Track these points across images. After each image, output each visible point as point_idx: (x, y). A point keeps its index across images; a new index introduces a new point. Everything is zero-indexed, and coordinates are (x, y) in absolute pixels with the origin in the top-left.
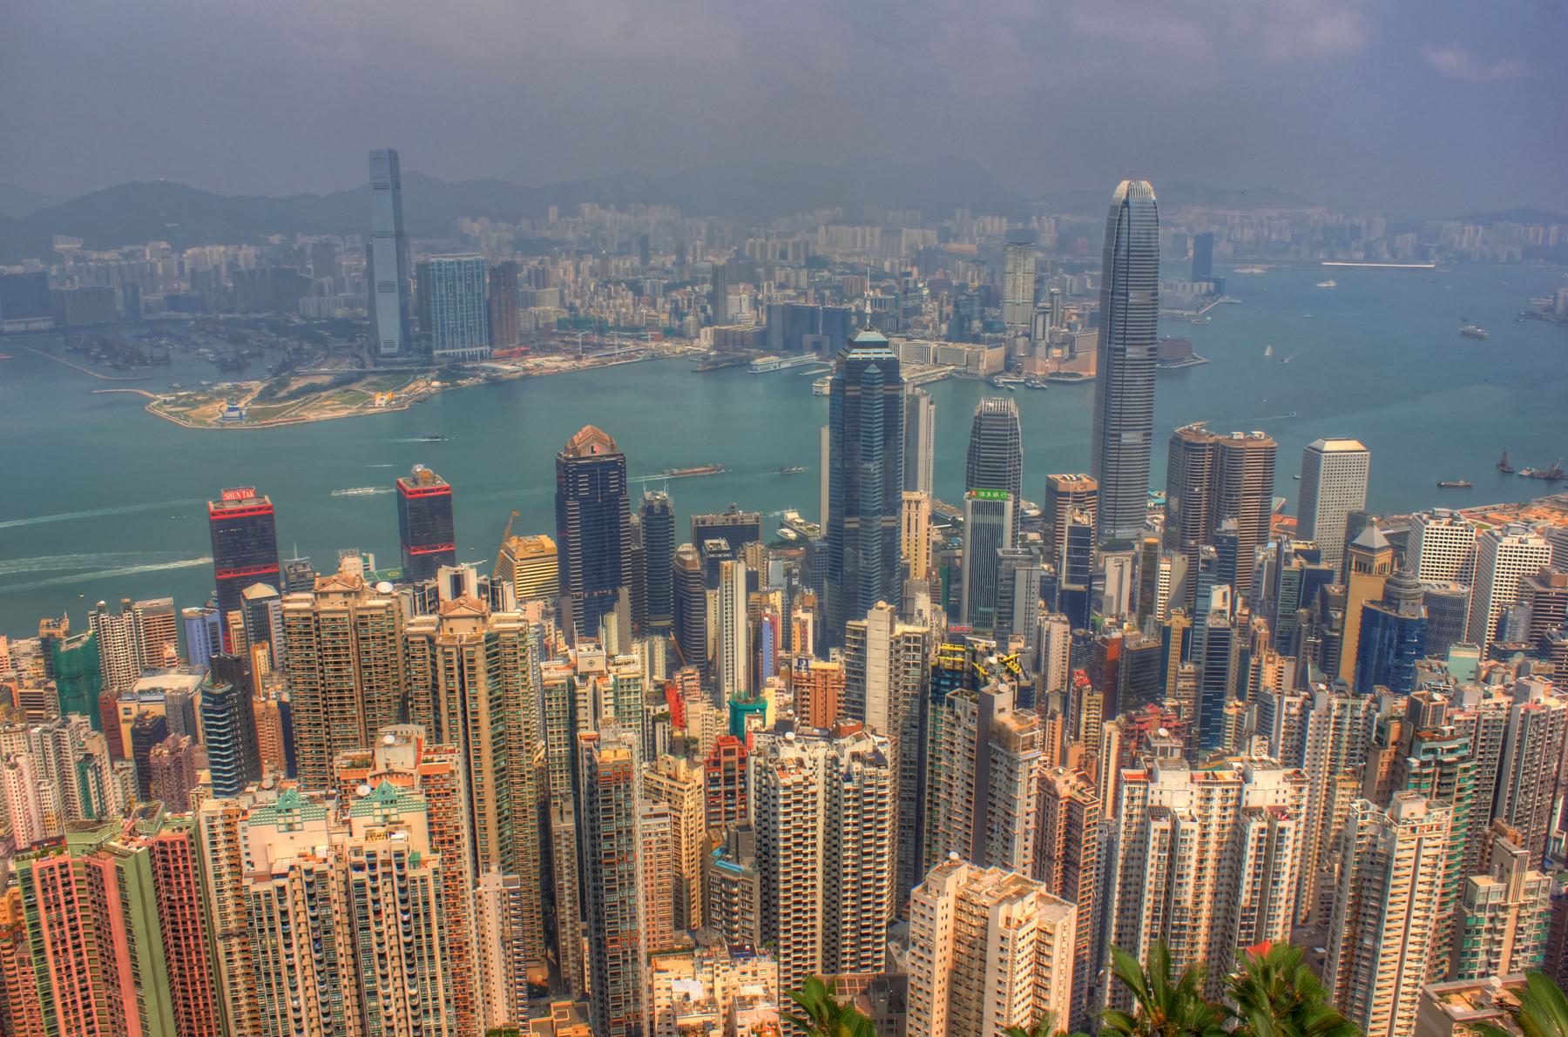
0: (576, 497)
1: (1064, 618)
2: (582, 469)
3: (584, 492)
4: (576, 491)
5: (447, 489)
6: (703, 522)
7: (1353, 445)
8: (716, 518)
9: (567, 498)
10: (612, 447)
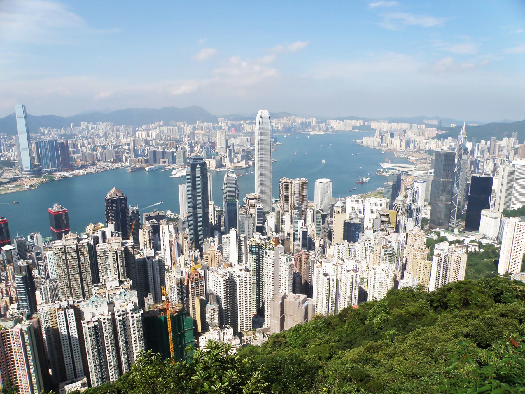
0: (112, 210)
1: (259, 233)
2: (114, 201)
3: (114, 208)
4: (112, 208)
5: (66, 211)
6: (147, 215)
7: (328, 180)
8: (151, 214)
9: (109, 210)
10: (123, 194)
